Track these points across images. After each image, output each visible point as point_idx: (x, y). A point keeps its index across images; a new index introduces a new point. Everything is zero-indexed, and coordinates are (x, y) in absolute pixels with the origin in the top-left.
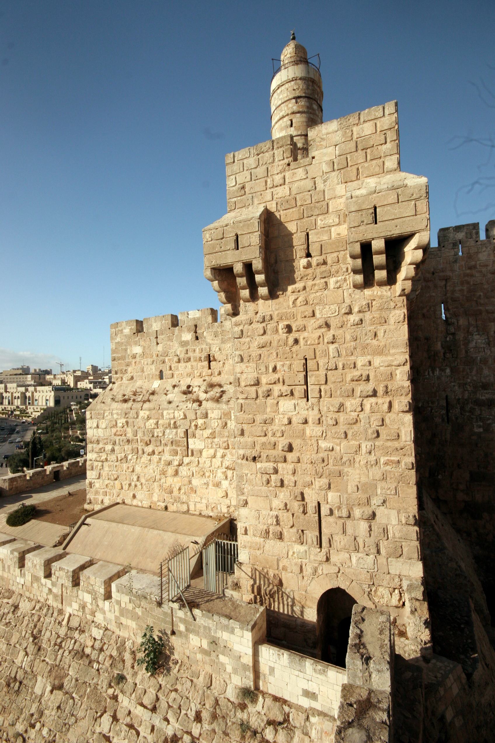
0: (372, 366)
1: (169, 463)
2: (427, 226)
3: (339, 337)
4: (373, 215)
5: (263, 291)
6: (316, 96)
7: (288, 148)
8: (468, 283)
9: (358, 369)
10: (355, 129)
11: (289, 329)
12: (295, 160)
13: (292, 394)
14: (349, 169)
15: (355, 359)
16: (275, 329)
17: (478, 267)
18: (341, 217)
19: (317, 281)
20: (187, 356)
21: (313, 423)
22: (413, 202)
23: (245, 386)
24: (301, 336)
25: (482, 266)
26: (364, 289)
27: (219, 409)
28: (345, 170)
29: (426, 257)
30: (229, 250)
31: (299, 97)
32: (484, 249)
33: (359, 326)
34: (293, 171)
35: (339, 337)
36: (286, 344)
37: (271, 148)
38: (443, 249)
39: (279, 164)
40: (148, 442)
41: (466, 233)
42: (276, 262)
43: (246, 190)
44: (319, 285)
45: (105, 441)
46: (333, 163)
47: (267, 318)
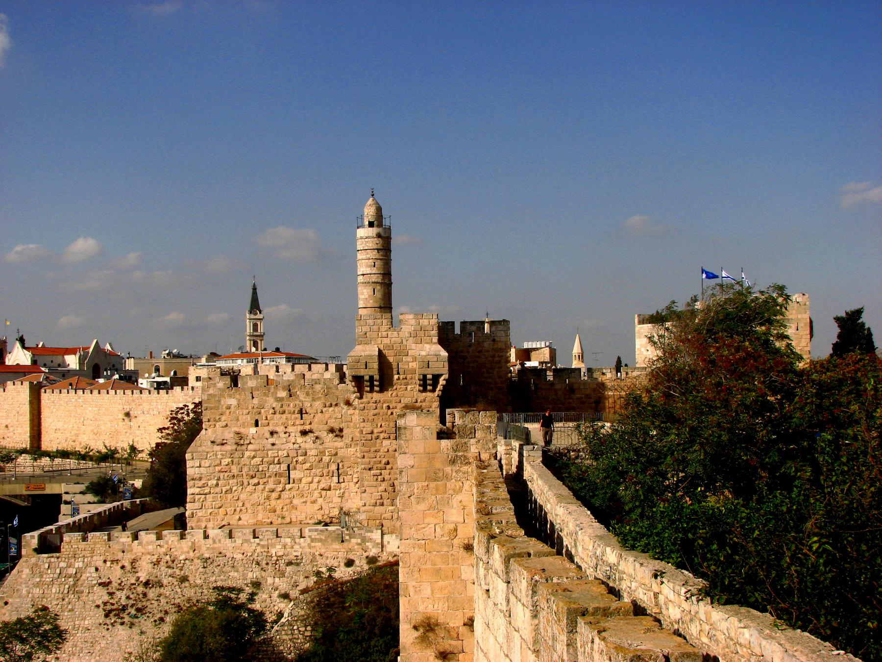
1: (273, 491)
10: (421, 320)
11: (389, 407)
13: (389, 438)
19: (402, 386)
27: (316, 449)
32: (487, 340)
39: (385, 327)
40: (254, 475)
45: (208, 477)
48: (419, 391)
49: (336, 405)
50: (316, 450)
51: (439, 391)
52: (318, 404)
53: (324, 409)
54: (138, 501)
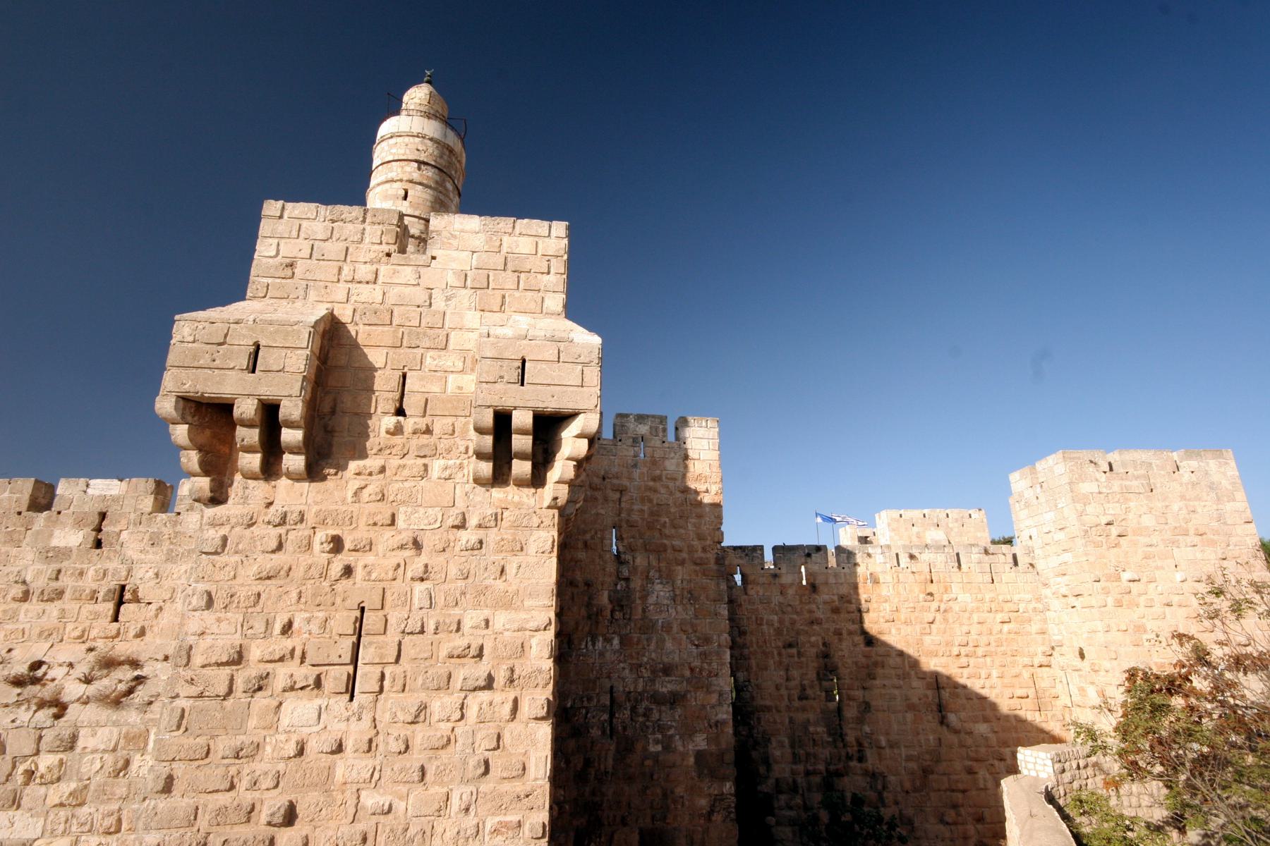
0: (490, 628)
2: (596, 406)
3: (435, 569)
4: (520, 371)
5: (294, 462)
6: (453, 172)
7: (392, 230)
8: (650, 501)
9: (463, 634)
10: (506, 239)
11: (337, 544)
12: (402, 250)
13: (318, 683)
14: (489, 291)
15: (461, 615)
16: (305, 542)
17: (664, 478)
18: (469, 361)
19: (408, 461)
20: (55, 585)
21: (356, 751)
22: (580, 367)
23: (203, 666)
25: (668, 479)
26: (492, 487)
28: (482, 291)
29: (593, 451)
30: (233, 368)
32: (672, 455)
33: (476, 552)
34: (394, 267)
35: (435, 569)
36: (324, 575)
37: (361, 219)
38: (619, 443)
41: (651, 428)
42: (333, 412)
43: (296, 271)
44: (411, 468)
46: (466, 275)
47: (292, 518)
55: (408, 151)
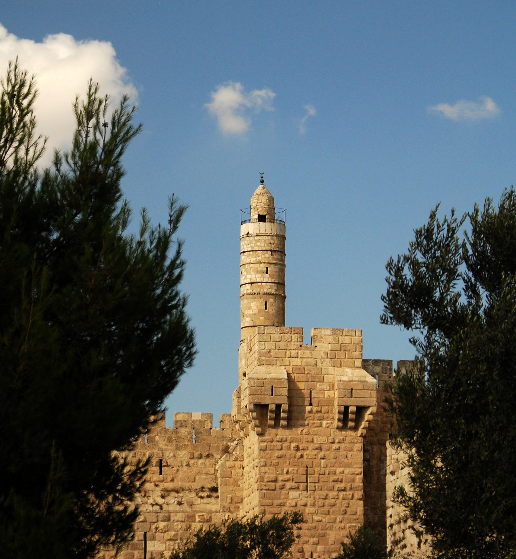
10: (340, 337)
11: (297, 449)
14: (336, 359)
18: (331, 386)
24: (305, 453)
27: (183, 512)
31: (275, 251)
36: (295, 457)
41: (382, 368)
44: (317, 423)
46: (328, 353)
48: (338, 428)
49: (208, 456)
50: (183, 514)
51: (364, 428)
52: (183, 455)
53: (192, 462)
54: (112, 477)
55: (266, 244)
